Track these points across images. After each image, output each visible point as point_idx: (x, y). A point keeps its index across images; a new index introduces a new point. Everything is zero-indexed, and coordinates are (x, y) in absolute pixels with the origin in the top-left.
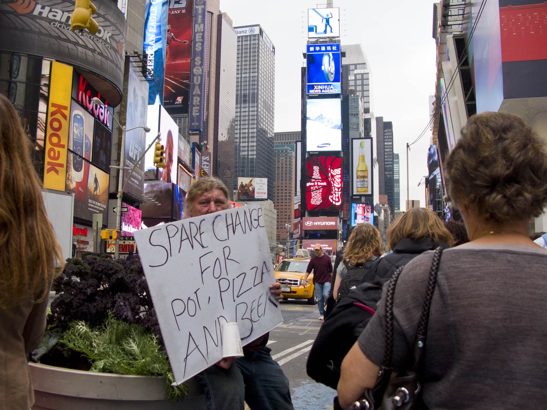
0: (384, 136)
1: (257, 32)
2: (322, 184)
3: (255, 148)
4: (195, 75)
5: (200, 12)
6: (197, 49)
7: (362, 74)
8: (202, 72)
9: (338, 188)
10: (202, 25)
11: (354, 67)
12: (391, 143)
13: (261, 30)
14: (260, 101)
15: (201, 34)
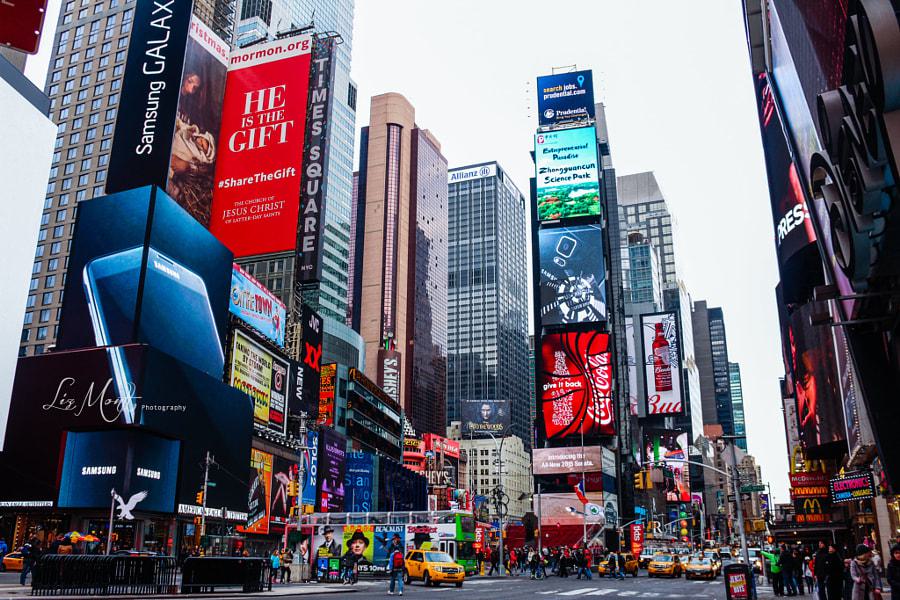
0: (710, 330)
1: (492, 171)
2: (573, 385)
3: (495, 355)
4: (309, 179)
5: (321, 69)
6: (314, 133)
7: (659, 218)
8: (322, 172)
9: (604, 392)
10: (324, 91)
11: (644, 207)
12: (722, 342)
13: (499, 170)
14: (501, 280)
15: (322, 106)
